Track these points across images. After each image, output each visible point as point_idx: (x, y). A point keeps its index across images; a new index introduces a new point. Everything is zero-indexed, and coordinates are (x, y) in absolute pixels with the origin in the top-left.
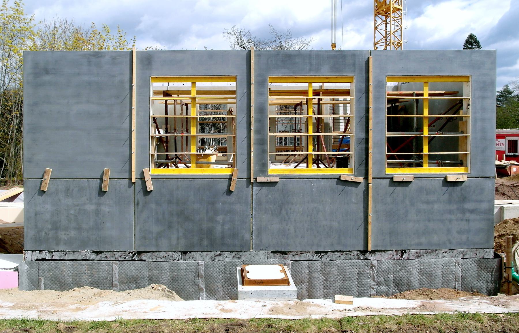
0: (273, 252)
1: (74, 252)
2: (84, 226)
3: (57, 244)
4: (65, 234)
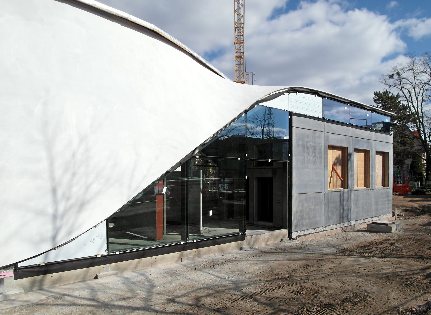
0: (356, 221)
1: (308, 230)
2: (311, 217)
3: (303, 227)
4: (305, 221)
